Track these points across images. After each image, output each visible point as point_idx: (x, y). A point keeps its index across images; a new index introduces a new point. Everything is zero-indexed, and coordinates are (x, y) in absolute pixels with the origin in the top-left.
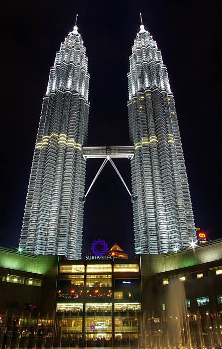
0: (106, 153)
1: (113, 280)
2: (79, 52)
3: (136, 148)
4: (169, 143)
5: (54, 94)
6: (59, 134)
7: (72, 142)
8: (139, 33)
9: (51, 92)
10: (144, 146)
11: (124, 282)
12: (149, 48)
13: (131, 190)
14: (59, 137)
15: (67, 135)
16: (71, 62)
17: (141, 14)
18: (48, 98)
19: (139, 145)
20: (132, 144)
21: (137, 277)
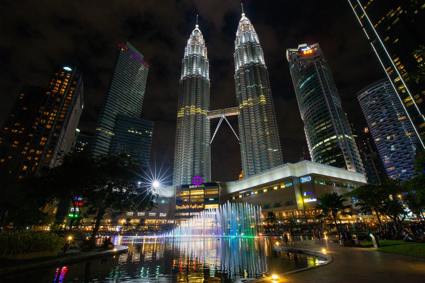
0: (222, 113)
1: (204, 198)
2: (199, 45)
3: (240, 108)
4: (262, 102)
5: (185, 79)
6: (190, 106)
7: (199, 110)
8: (241, 20)
9: (184, 78)
10: (245, 106)
11: (210, 199)
12: (247, 32)
13: (238, 136)
14: (190, 108)
15: (196, 106)
16: (194, 54)
17: (242, 4)
18: (182, 82)
19: (242, 106)
20: (238, 105)
21: (218, 196)
